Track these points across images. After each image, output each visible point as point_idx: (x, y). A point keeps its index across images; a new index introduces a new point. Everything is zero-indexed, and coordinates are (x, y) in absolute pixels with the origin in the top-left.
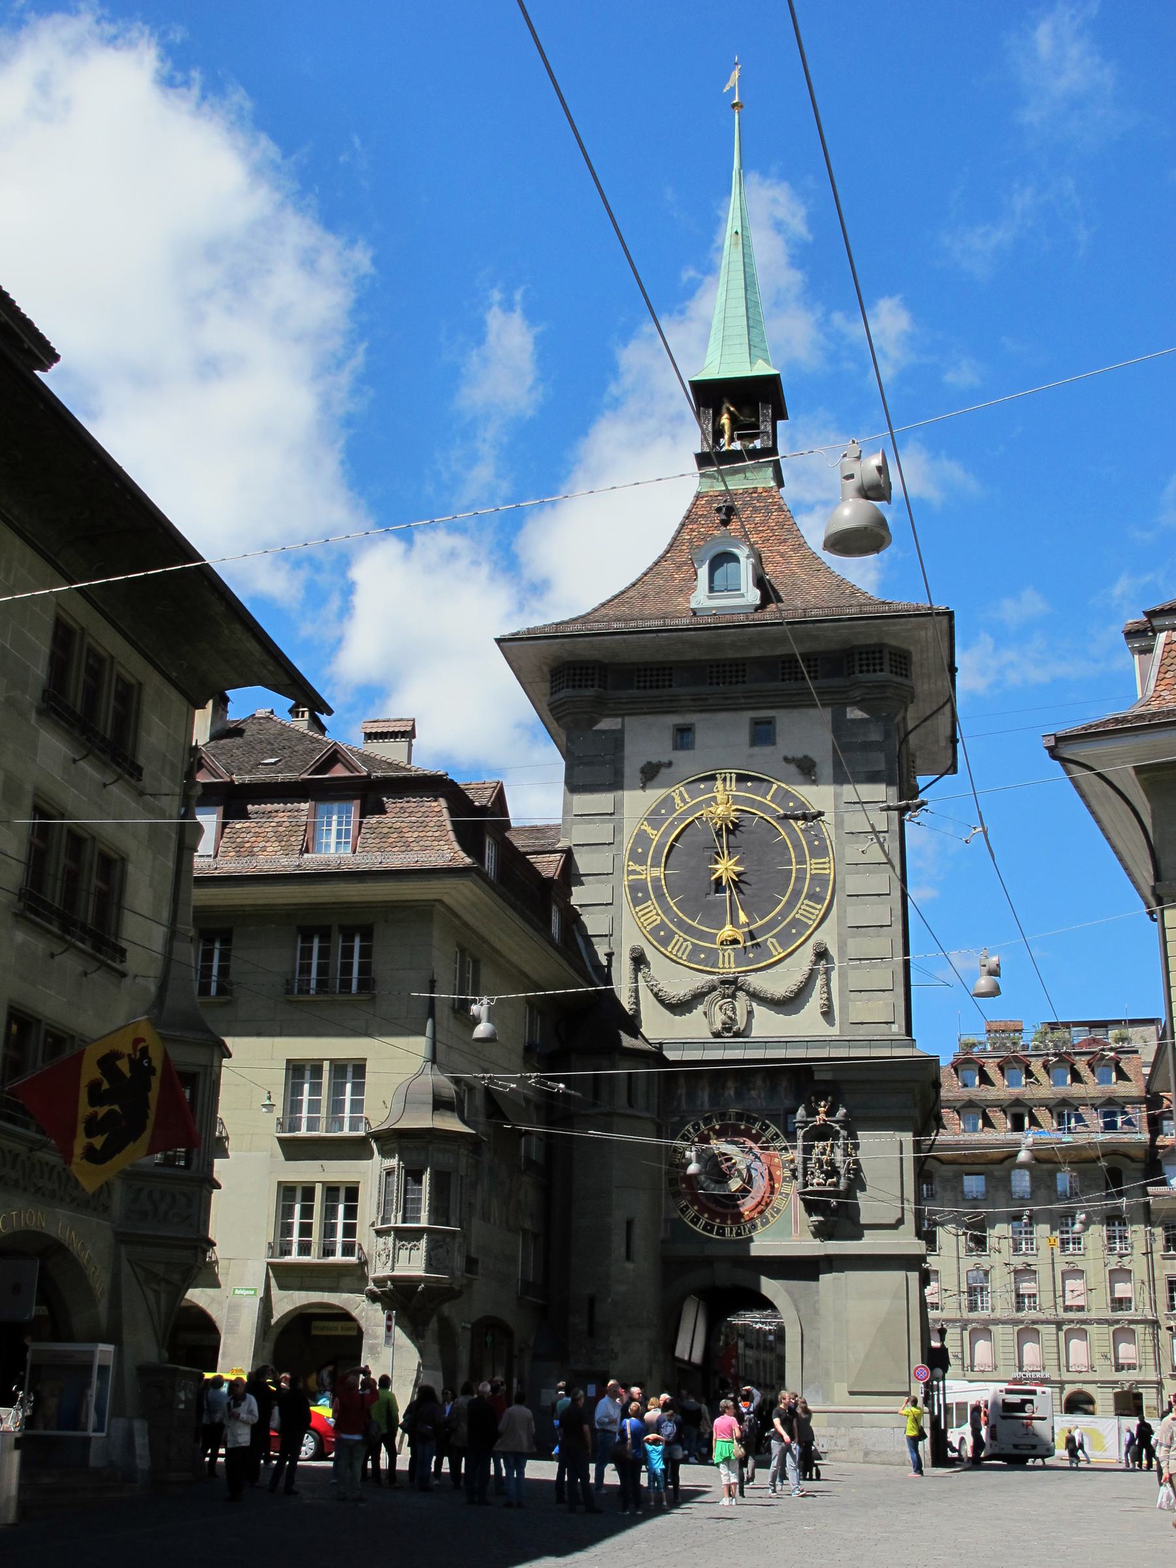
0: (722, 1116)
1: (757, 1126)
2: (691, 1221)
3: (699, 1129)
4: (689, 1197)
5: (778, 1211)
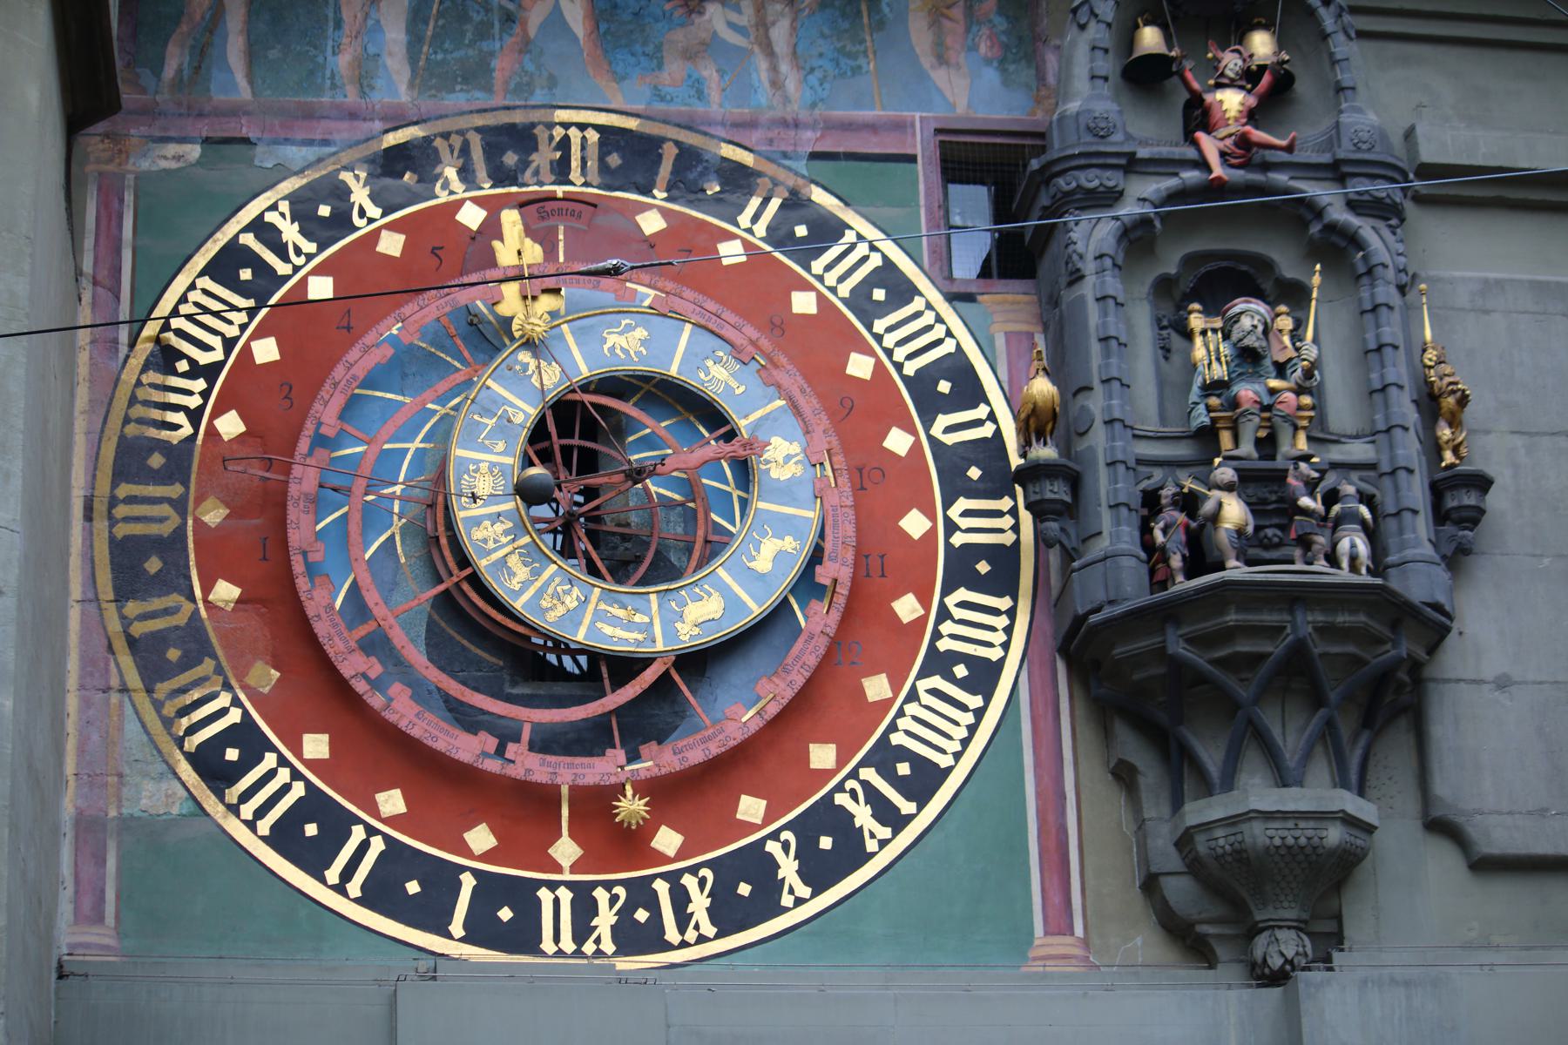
0: (507, 149)
1: (756, 218)
2: (284, 838)
3: (341, 222)
4: (267, 676)
5: (925, 780)
